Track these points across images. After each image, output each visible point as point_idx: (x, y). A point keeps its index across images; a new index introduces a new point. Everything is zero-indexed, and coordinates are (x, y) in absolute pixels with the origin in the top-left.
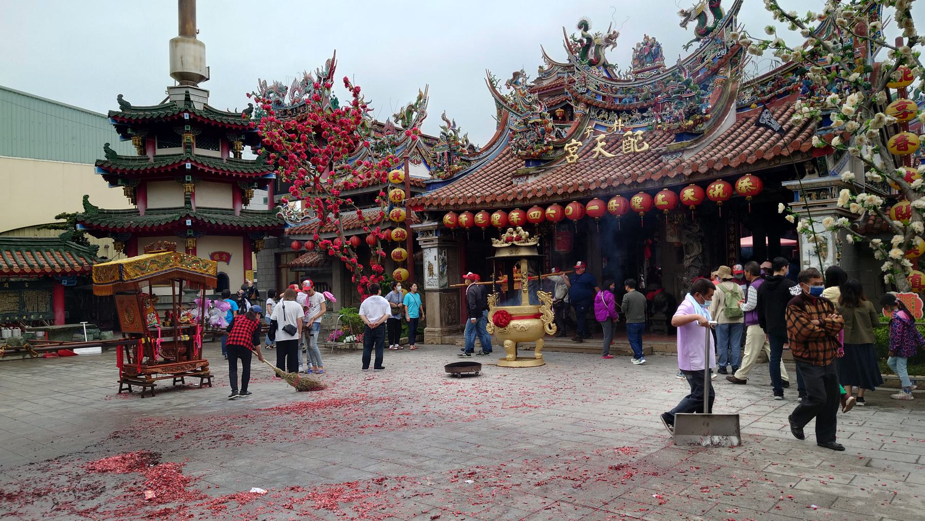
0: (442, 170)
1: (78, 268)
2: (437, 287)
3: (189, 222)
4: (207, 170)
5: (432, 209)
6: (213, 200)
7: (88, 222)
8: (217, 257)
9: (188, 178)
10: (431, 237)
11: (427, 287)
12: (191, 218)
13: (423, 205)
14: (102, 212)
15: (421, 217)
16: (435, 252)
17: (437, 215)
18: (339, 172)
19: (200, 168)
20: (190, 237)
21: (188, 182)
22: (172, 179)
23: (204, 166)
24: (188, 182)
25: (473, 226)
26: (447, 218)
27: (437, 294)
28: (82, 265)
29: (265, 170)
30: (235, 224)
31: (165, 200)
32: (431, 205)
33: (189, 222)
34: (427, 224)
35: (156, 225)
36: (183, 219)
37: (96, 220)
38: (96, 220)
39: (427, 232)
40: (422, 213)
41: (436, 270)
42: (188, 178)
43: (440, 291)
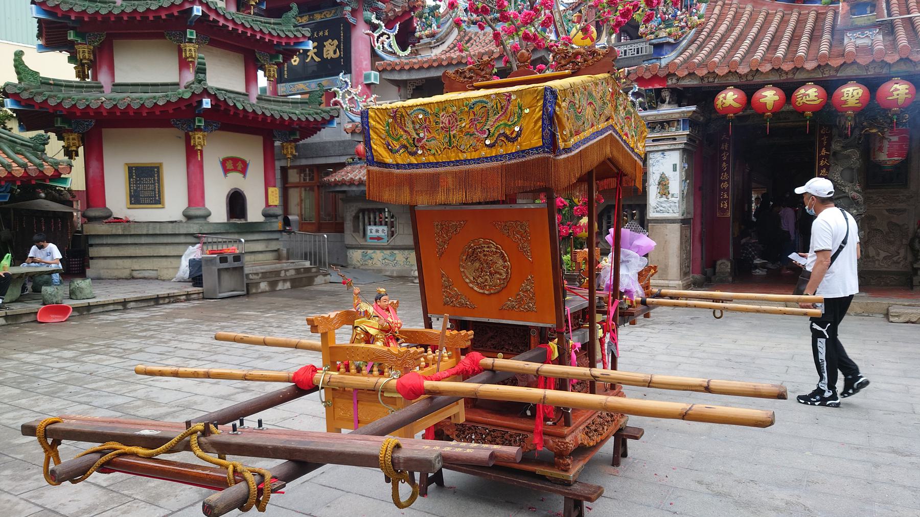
0: (669, 26)
1: (18, 172)
2: (677, 215)
3: (207, 103)
4: (222, 22)
5: (687, 82)
6: (224, 77)
7: (25, 96)
8: (229, 165)
9: (191, 34)
10: (672, 132)
11: (652, 214)
12: (209, 95)
13: (671, 75)
14: (46, 82)
15: (656, 99)
16: (675, 158)
17: (702, 95)
18: (428, 40)
19: (213, 16)
20: (199, 129)
21: (190, 41)
22: (161, 36)
23: (218, 14)
24: (190, 41)
25: (788, 112)
26: (729, 98)
27: (677, 226)
28: (24, 166)
29: (299, 35)
30: (268, 114)
31: (144, 71)
32: (691, 75)
33: (207, 103)
34: (667, 110)
35: (149, 105)
36: (196, 99)
37: (41, 94)
38: (41, 94)
39: (663, 124)
40: (658, 92)
41: (676, 185)
42: (191, 34)
43: (684, 222)
